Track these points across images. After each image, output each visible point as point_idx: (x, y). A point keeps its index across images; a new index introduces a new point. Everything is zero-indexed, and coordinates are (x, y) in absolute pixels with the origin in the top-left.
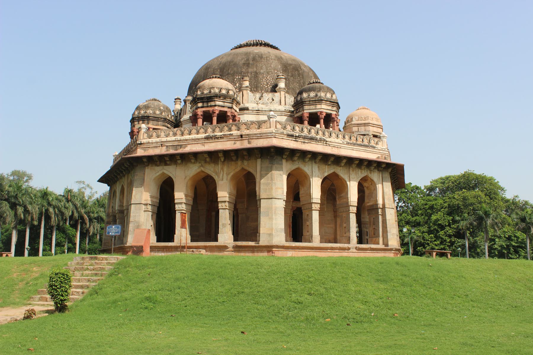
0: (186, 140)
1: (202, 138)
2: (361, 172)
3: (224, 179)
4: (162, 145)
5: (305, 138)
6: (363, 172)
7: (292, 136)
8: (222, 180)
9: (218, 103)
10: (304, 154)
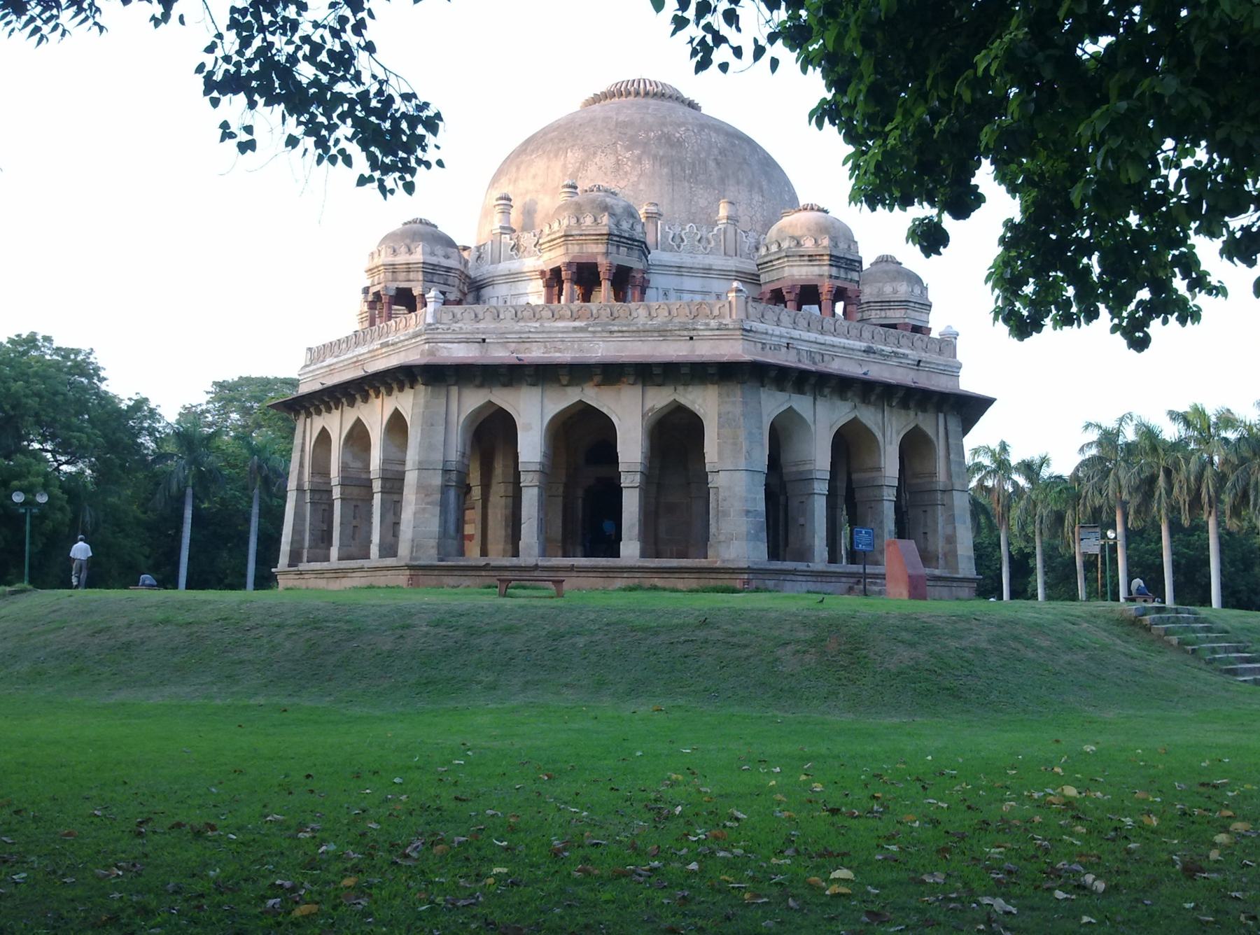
0: (833, 346)
1: (860, 351)
3: (893, 442)
4: (788, 344)
8: (891, 444)
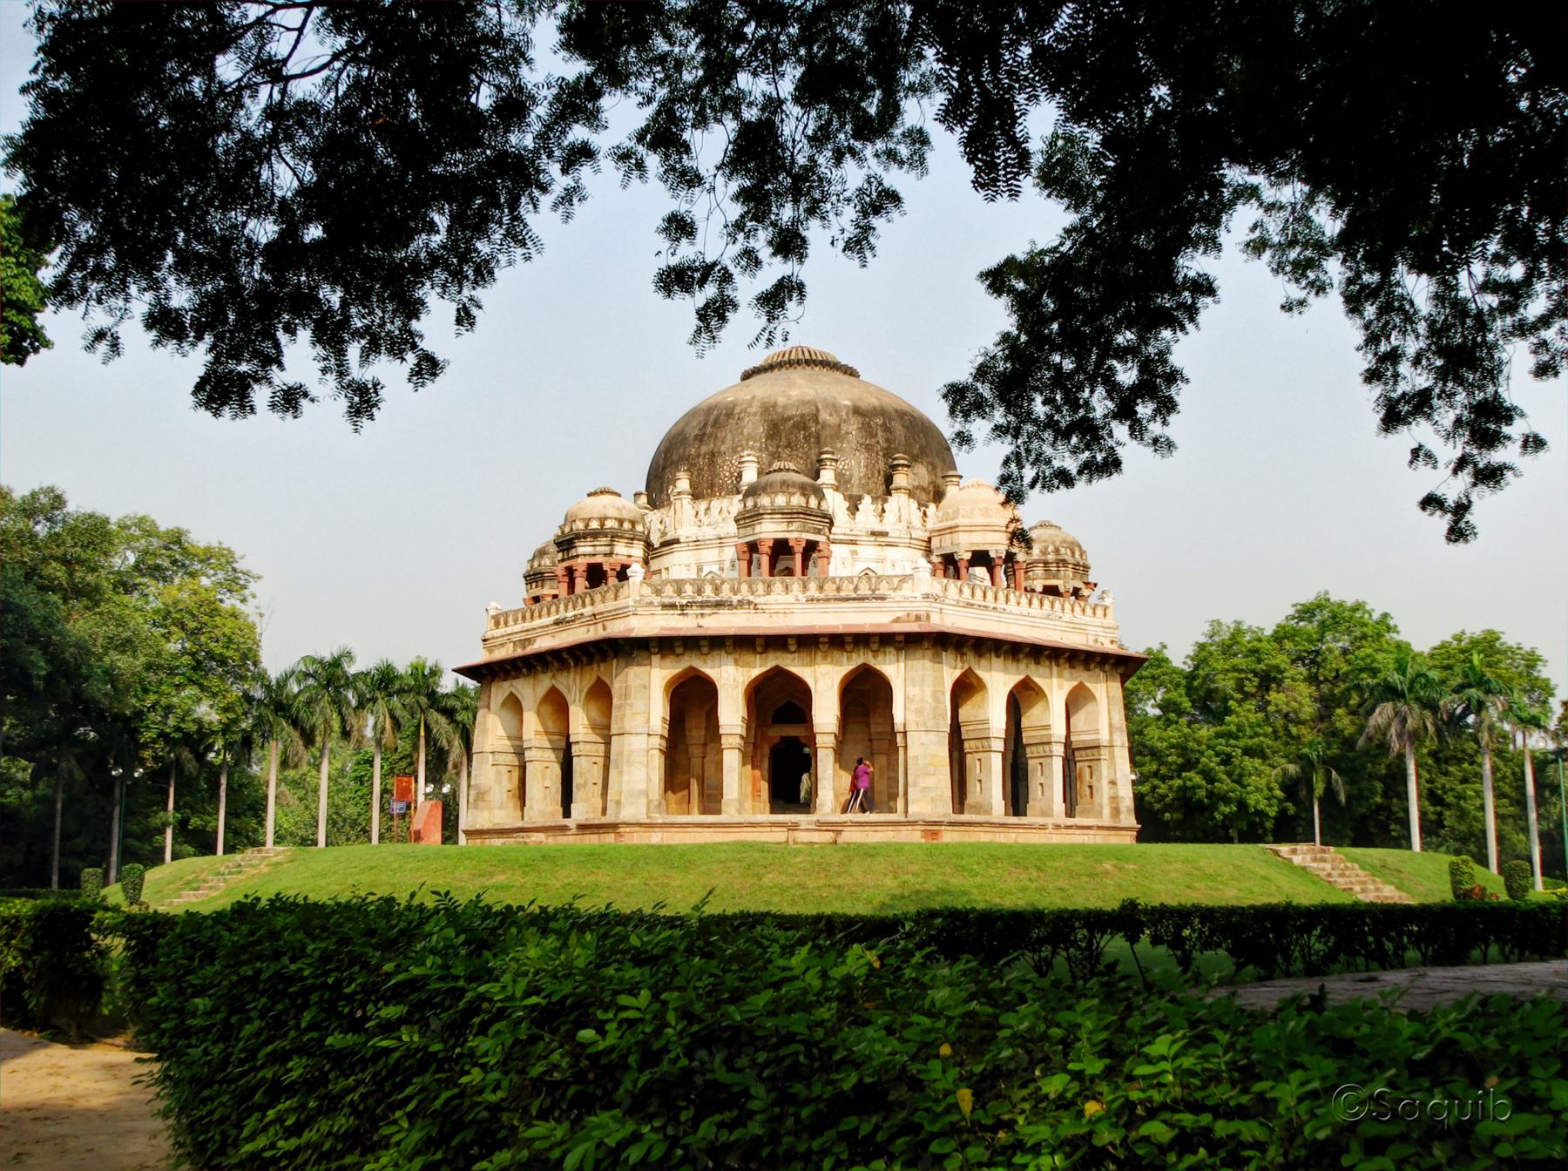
2: (849, 659)
5: (702, 605)
6: (854, 656)
7: (673, 606)
9: (581, 550)
10: (691, 643)
